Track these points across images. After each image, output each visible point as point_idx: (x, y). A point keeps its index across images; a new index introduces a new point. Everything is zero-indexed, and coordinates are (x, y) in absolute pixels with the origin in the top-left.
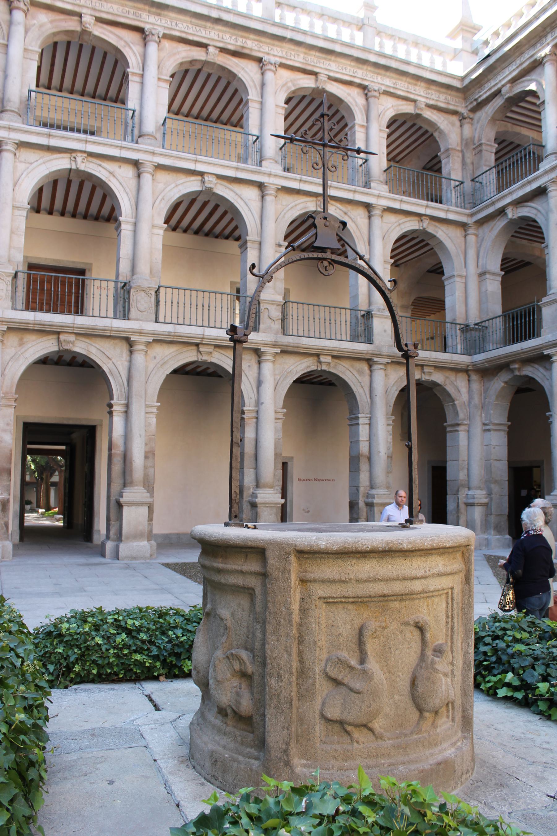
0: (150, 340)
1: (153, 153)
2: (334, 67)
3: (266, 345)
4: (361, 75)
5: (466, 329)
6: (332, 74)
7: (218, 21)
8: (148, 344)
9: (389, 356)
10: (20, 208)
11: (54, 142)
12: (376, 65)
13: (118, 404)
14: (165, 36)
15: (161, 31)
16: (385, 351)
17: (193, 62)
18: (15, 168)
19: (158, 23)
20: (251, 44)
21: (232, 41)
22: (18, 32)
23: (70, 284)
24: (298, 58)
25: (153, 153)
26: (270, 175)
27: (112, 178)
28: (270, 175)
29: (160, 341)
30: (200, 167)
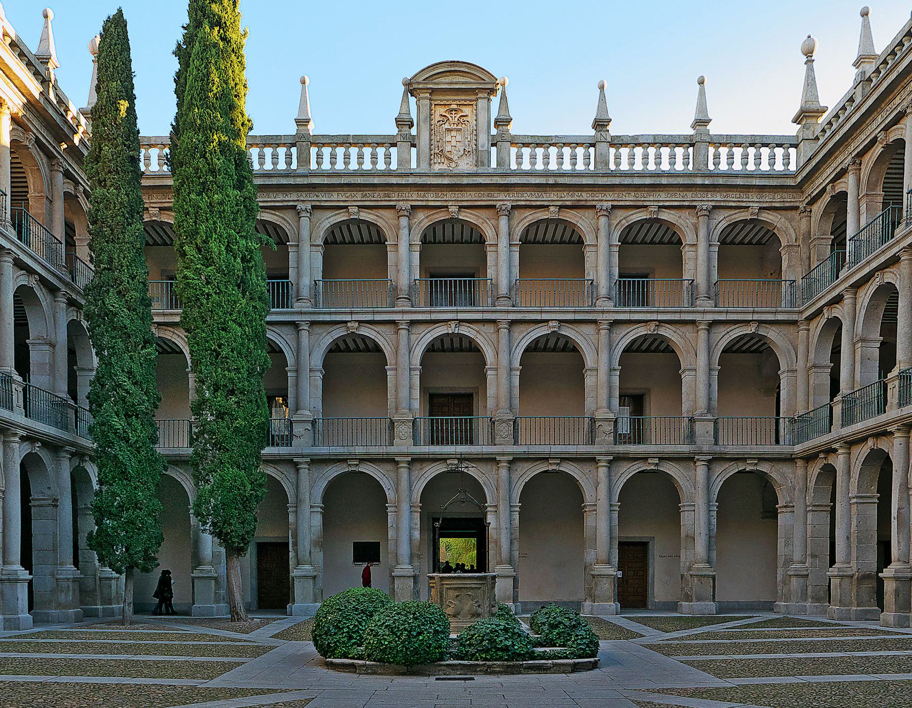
0: (511, 458)
1: (508, 312)
2: (663, 197)
3: (601, 454)
4: (689, 197)
5: (792, 421)
6: (661, 204)
7: (555, 185)
8: (510, 462)
9: (709, 454)
10: (415, 369)
11: (434, 317)
12: (703, 186)
13: (491, 506)
14: (513, 207)
15: (509, 204)
16: (705, 449)
17: (539, 222)
18: (409, 339)
19: (508, 198)
20: (585, 196)
21: (568, 197)
22: (404, 232)
23: (451, 423)
24: (629, 198)
25: (508, 312)
26: (603, 312)
27: (478, 336)
28: (603, 312)
29: (516, 460)
30: (545, 317)
